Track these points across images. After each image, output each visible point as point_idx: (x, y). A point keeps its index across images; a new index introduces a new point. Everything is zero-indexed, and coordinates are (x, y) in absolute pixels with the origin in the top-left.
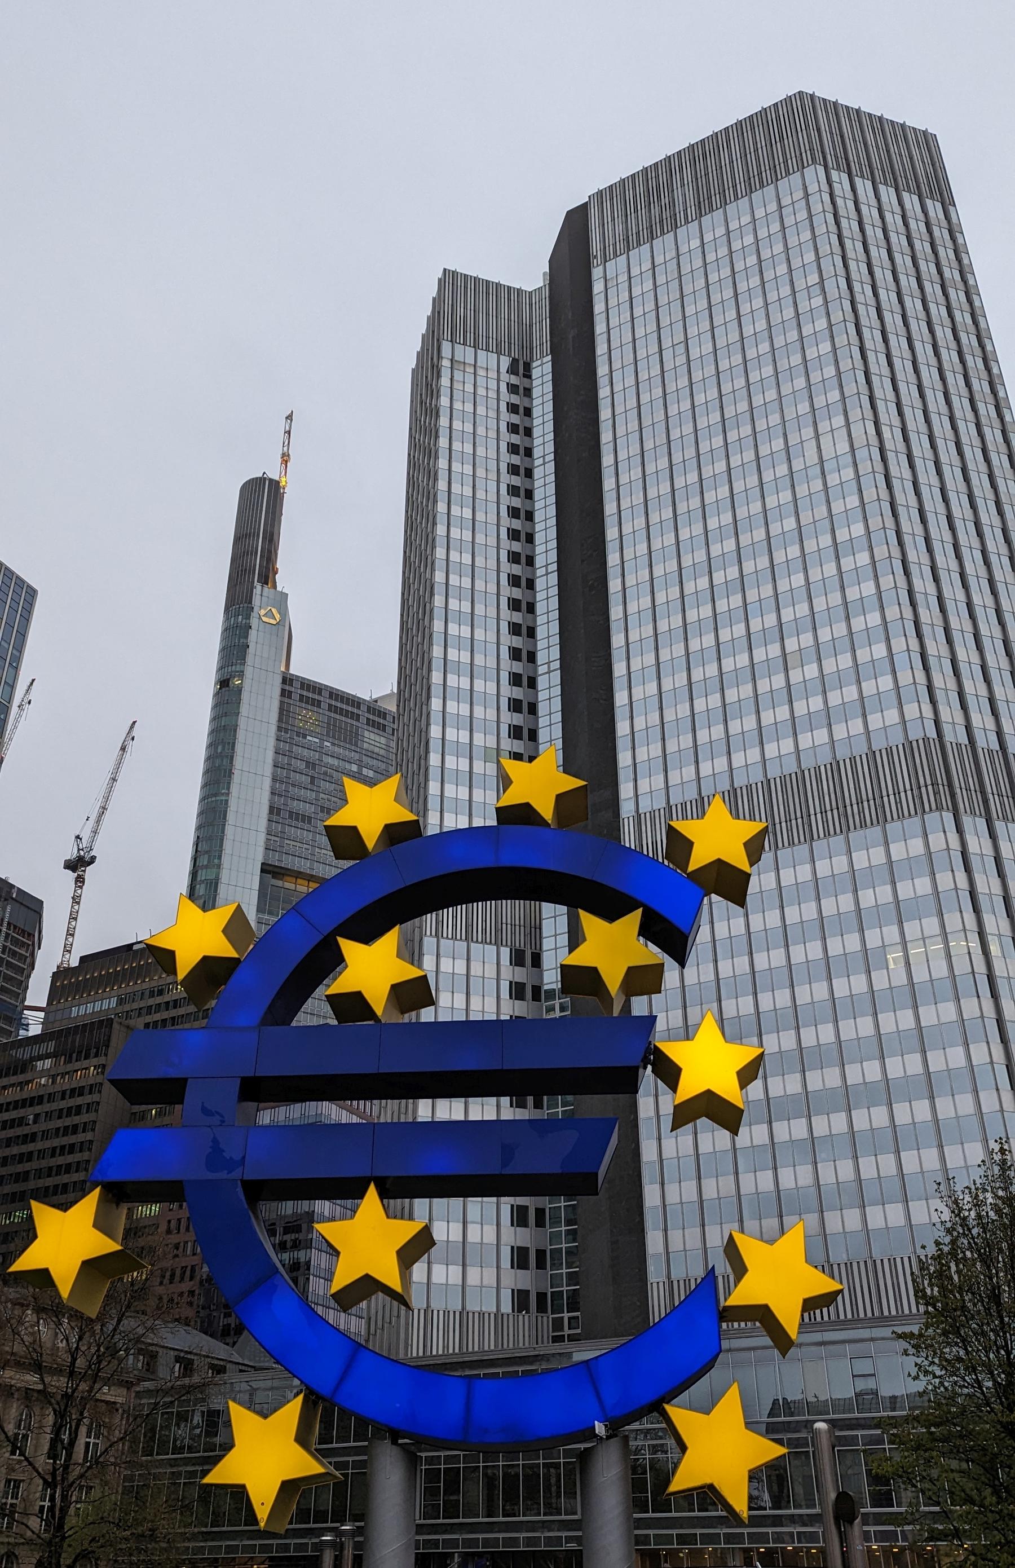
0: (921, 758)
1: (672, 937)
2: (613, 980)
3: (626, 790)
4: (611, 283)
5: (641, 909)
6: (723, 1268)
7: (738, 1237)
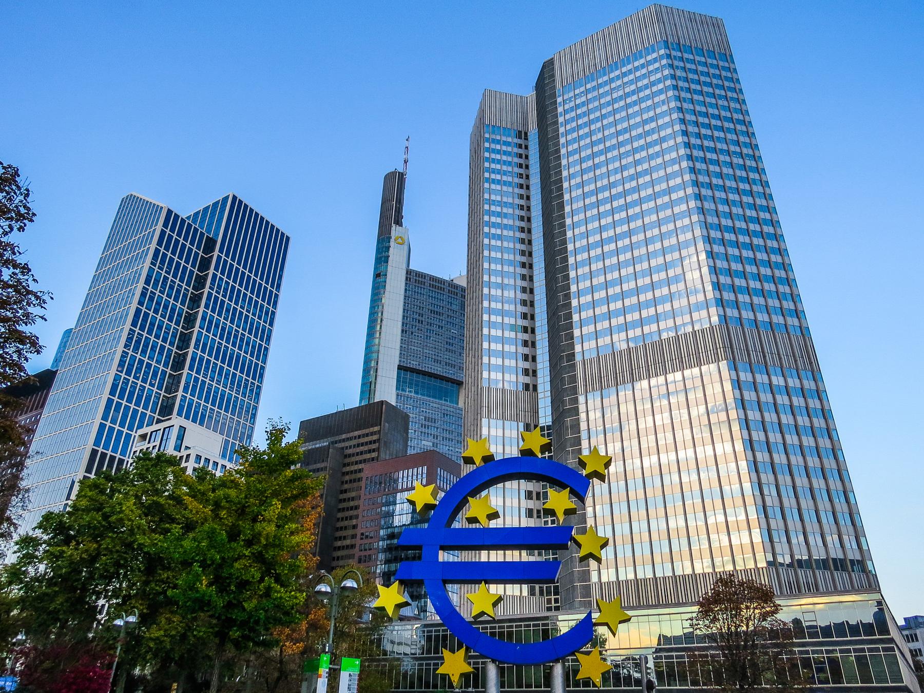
0: (718, 335)
1: (579, 495)
3: (578, 348)
4: (566, 103)
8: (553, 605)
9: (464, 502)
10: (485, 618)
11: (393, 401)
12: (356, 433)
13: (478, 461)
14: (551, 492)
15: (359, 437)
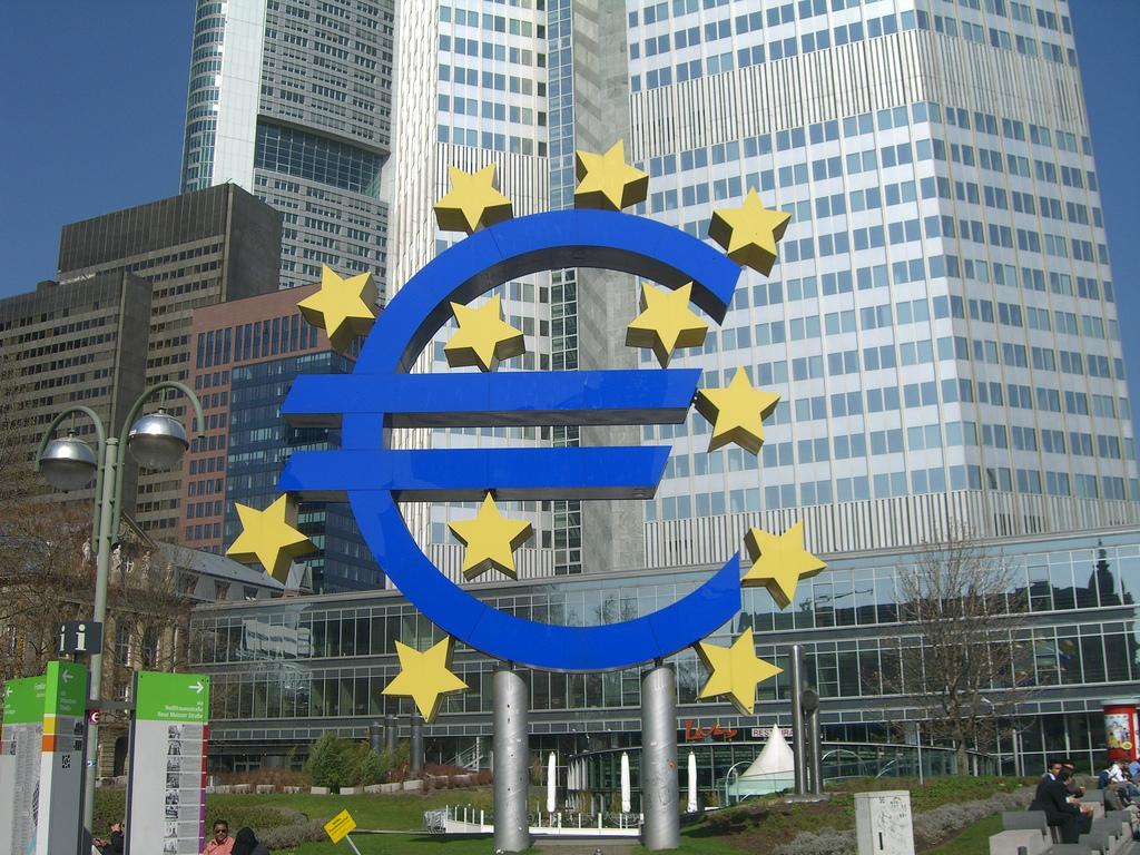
1: (713, 302)
2: (669, 342)
5: (691, 283)
6: (744, 555)
7: (756, 532)
8: (568, 563)
9: (441, 315)
10: (490, 578)
11: (248, 185)
12: (176, 250)
13: (474, 220)
14: (655, 291)
15: (183, 256)
